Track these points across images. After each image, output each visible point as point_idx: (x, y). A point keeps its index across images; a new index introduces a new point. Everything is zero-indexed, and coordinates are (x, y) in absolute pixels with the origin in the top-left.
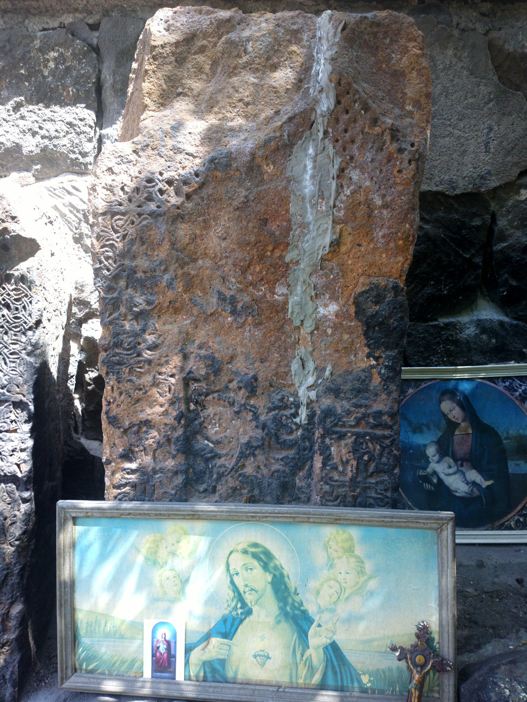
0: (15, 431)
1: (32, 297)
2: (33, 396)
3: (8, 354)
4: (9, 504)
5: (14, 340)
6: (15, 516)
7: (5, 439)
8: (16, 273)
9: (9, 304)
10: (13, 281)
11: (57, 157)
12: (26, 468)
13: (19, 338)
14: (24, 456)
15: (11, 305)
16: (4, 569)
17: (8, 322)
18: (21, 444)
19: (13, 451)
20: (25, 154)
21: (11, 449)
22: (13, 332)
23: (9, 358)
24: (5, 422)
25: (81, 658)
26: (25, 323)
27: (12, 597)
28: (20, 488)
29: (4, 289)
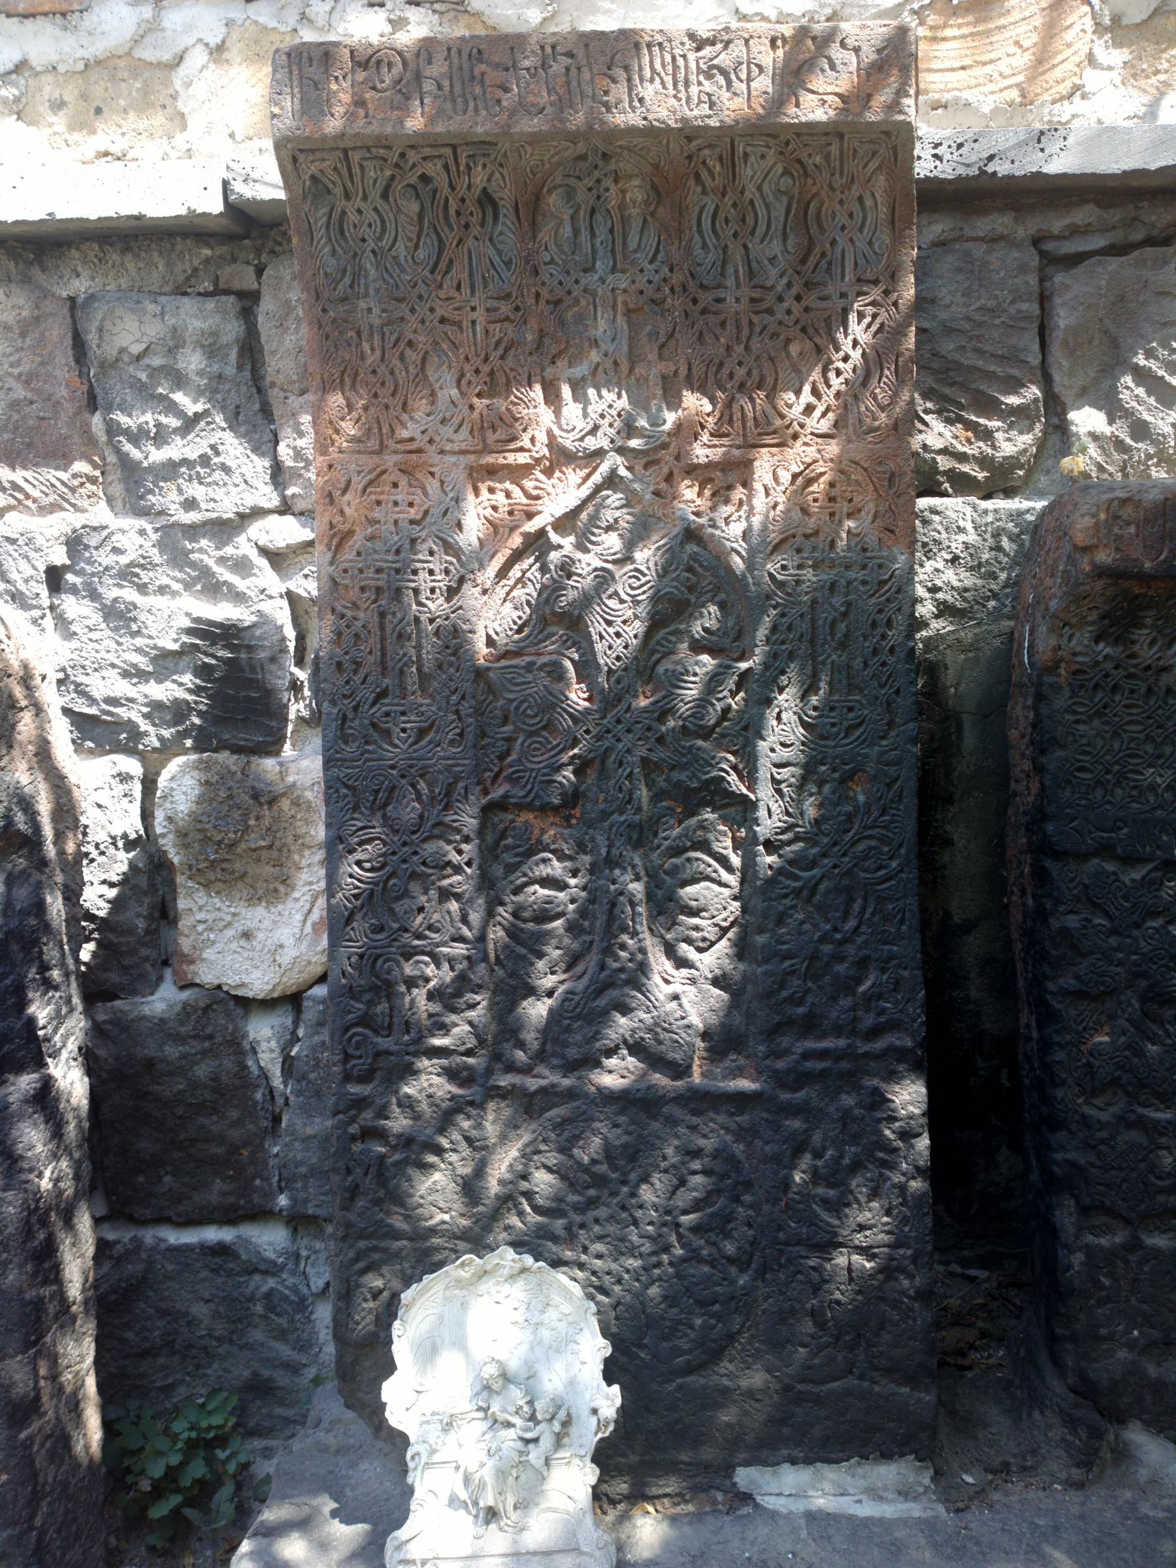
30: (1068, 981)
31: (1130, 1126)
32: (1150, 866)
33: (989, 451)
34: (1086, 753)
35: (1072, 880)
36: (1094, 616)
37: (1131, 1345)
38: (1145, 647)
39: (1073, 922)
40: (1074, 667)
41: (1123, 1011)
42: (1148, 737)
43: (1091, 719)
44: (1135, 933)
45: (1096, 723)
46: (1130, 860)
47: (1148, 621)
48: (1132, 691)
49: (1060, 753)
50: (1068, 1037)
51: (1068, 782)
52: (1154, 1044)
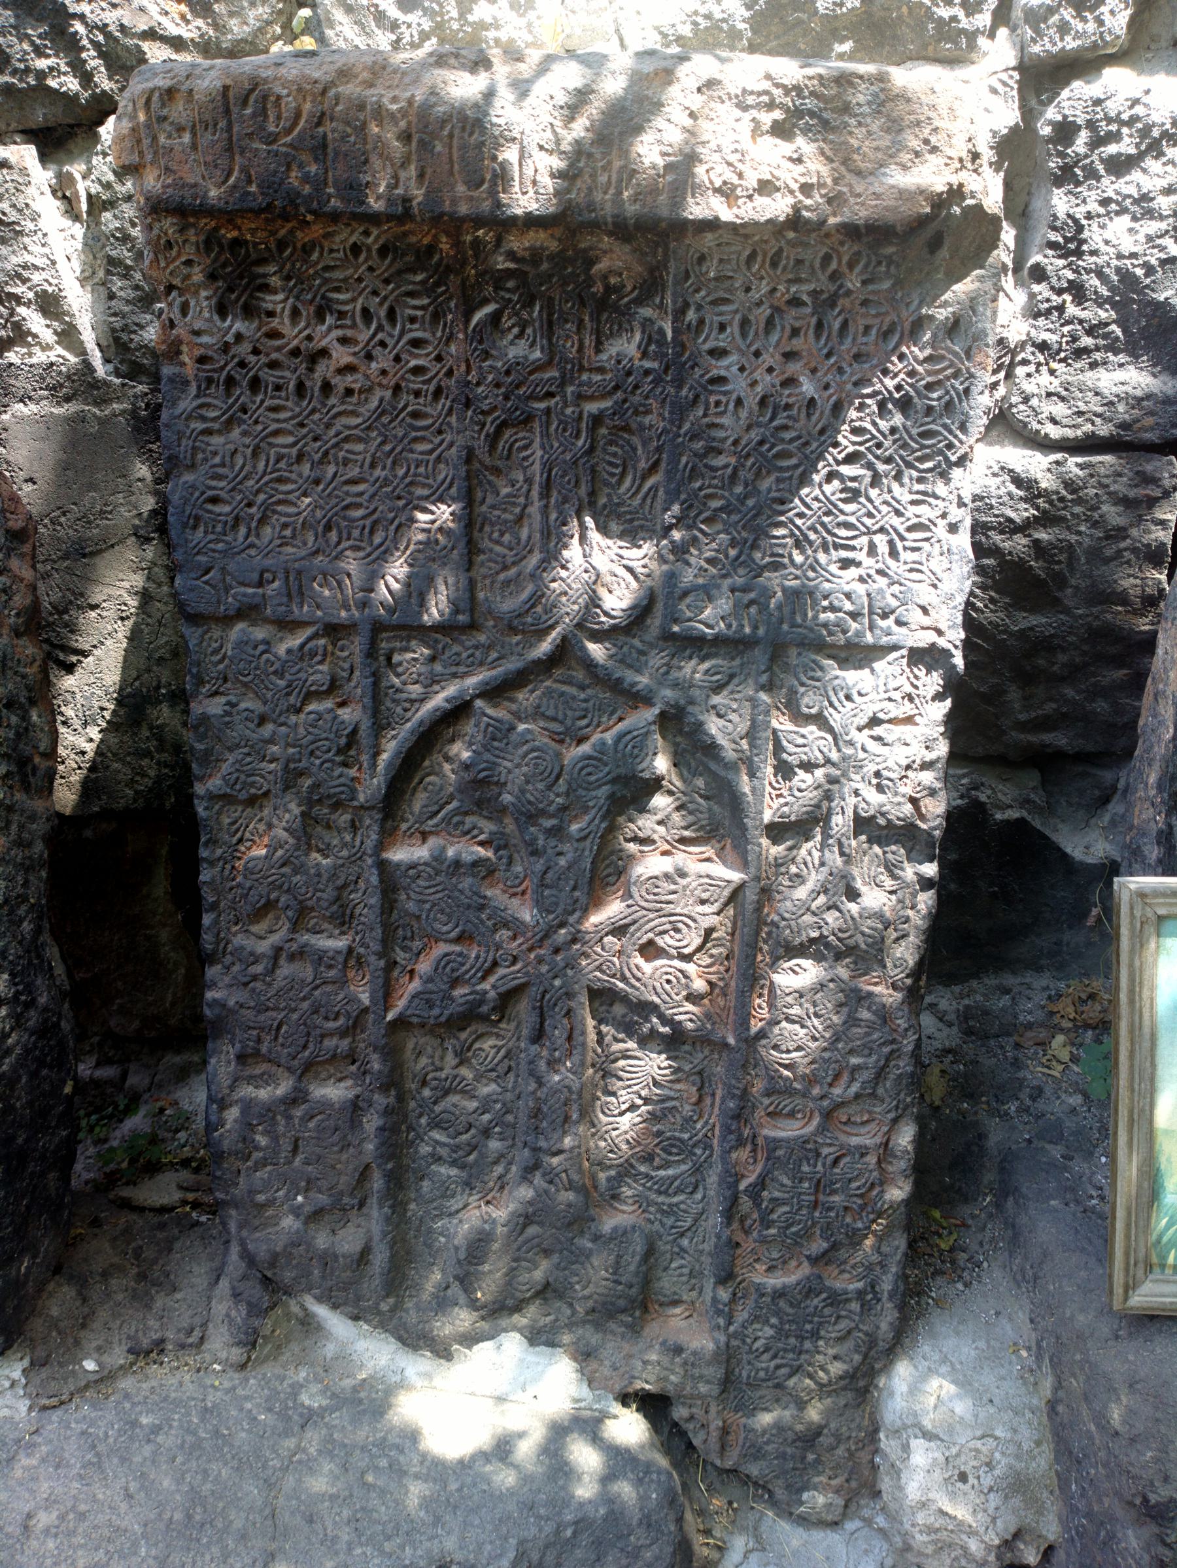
0: (909, 720)
1: (972, 376)
2: (963, 635)
3: (901, 529)
4: (891, 893)
5: (918, 493)
6: (907, 920)
7: (889, 738)
8: (942, 314)
9: (911, 398)
10: (928, 336)
11: (899, 17)
12: (936, 808)
13: (928, 488)
14: (928, 778)
15: (916, 400)
16: (883, 1044)
17: (905, 446)
18: (926, 752)
19: (908, 767)
20: (822, 11)
21: (904, 763)
22: (915, 474)
23: (902, 539)
24: (890, 699)
25: (1165, 1239)
26: (950, 446)
27: (897, 1107)
28: (913, 854)
29: (902, 357)
30: (215, 783)
31: (292, 957)
32: (309, 631)
33: (211, 33)
34: (220, 477)
35: (216, 652)
36: (198, 277)
37: (296, 1211)
38: (287, 321)
39: (215, 707)
40: (198, 352)
41: (280, 820)
42: (300, 457)
43: (229, 424)
44: (293, 718)
45: (236, 433)
46: (287, 625)
47: (274, 281)
48: (278, 388)
49: (189, 477)
50: (219, 852)
51: (197, 518)
52: (326, 857)
